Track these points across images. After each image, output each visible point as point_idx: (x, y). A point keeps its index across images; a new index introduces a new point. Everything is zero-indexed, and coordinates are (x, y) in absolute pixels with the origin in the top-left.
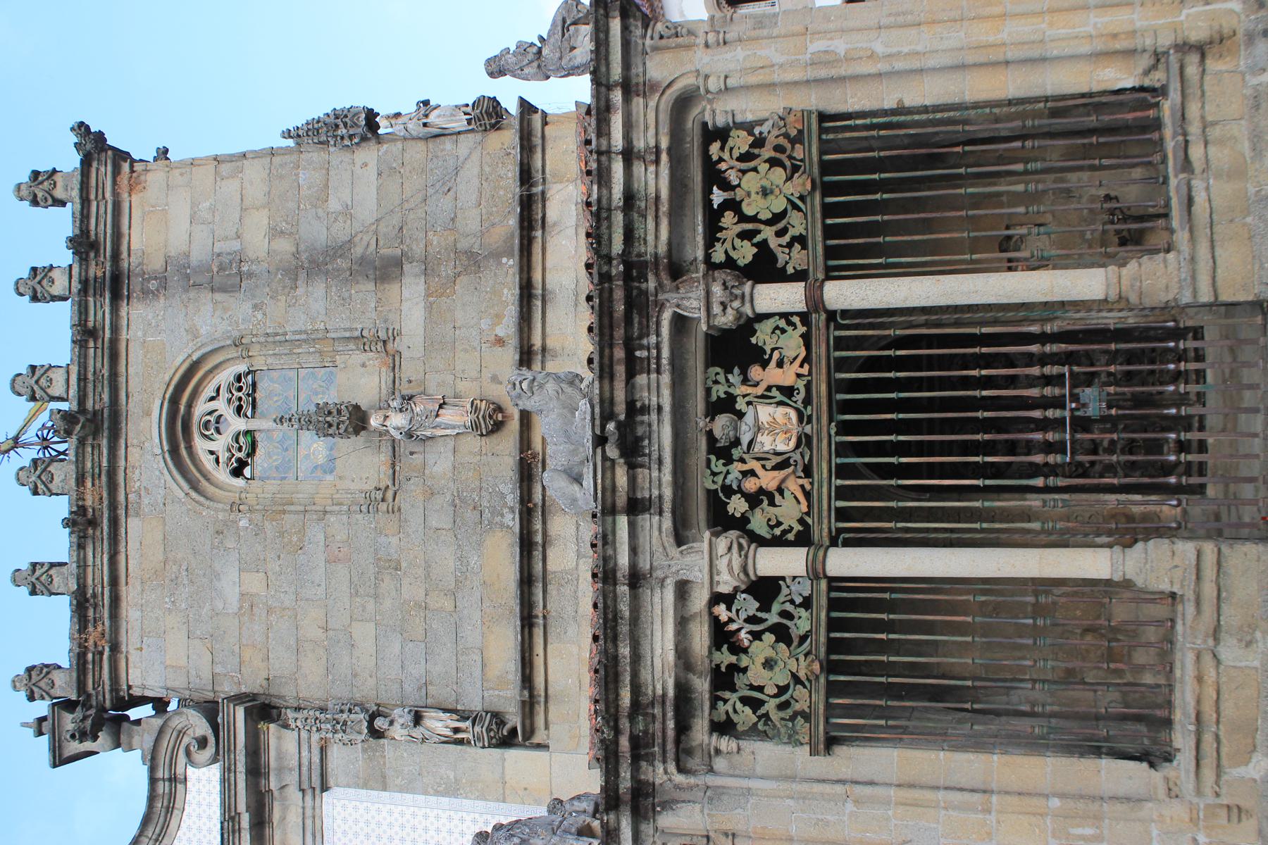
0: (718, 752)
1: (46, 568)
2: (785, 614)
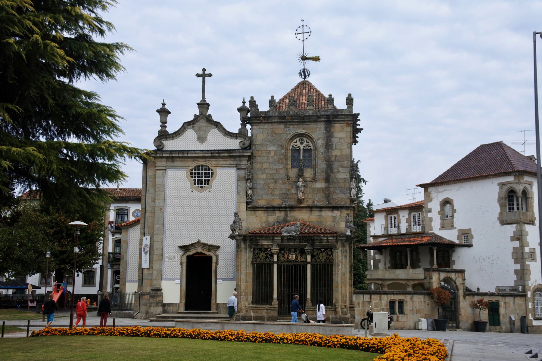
0: (251, 249)
2: (269, 258)
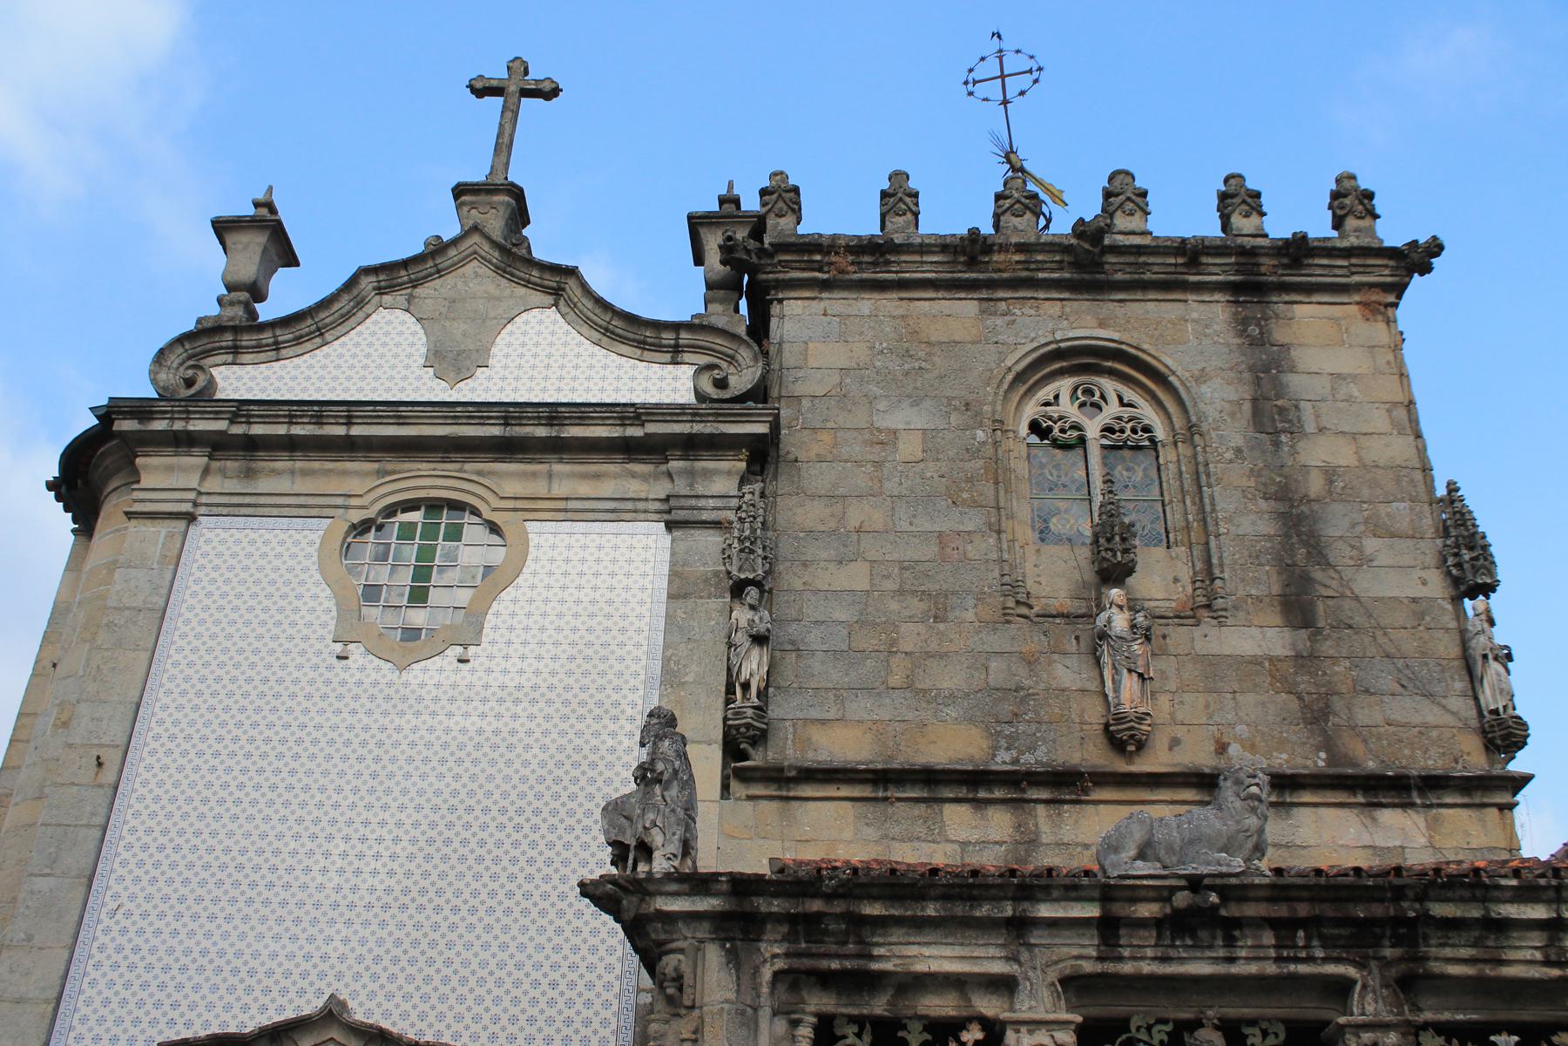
0: (795, 1024)
1: (914, 209)
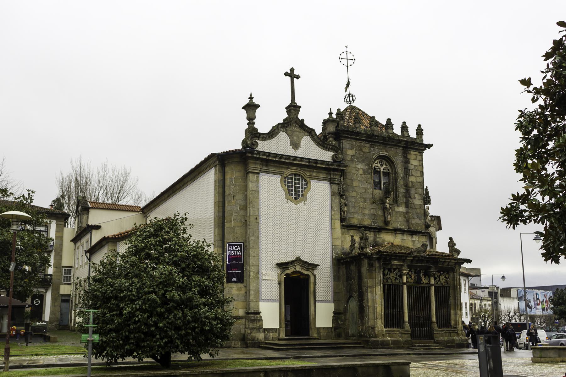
2: (398, 279)
